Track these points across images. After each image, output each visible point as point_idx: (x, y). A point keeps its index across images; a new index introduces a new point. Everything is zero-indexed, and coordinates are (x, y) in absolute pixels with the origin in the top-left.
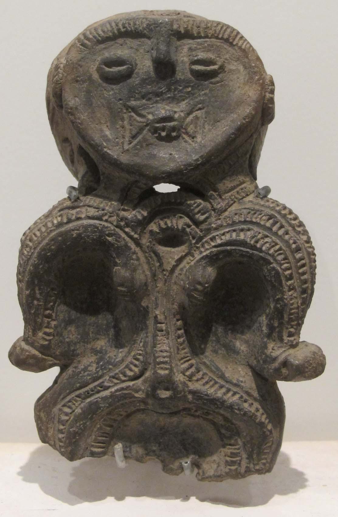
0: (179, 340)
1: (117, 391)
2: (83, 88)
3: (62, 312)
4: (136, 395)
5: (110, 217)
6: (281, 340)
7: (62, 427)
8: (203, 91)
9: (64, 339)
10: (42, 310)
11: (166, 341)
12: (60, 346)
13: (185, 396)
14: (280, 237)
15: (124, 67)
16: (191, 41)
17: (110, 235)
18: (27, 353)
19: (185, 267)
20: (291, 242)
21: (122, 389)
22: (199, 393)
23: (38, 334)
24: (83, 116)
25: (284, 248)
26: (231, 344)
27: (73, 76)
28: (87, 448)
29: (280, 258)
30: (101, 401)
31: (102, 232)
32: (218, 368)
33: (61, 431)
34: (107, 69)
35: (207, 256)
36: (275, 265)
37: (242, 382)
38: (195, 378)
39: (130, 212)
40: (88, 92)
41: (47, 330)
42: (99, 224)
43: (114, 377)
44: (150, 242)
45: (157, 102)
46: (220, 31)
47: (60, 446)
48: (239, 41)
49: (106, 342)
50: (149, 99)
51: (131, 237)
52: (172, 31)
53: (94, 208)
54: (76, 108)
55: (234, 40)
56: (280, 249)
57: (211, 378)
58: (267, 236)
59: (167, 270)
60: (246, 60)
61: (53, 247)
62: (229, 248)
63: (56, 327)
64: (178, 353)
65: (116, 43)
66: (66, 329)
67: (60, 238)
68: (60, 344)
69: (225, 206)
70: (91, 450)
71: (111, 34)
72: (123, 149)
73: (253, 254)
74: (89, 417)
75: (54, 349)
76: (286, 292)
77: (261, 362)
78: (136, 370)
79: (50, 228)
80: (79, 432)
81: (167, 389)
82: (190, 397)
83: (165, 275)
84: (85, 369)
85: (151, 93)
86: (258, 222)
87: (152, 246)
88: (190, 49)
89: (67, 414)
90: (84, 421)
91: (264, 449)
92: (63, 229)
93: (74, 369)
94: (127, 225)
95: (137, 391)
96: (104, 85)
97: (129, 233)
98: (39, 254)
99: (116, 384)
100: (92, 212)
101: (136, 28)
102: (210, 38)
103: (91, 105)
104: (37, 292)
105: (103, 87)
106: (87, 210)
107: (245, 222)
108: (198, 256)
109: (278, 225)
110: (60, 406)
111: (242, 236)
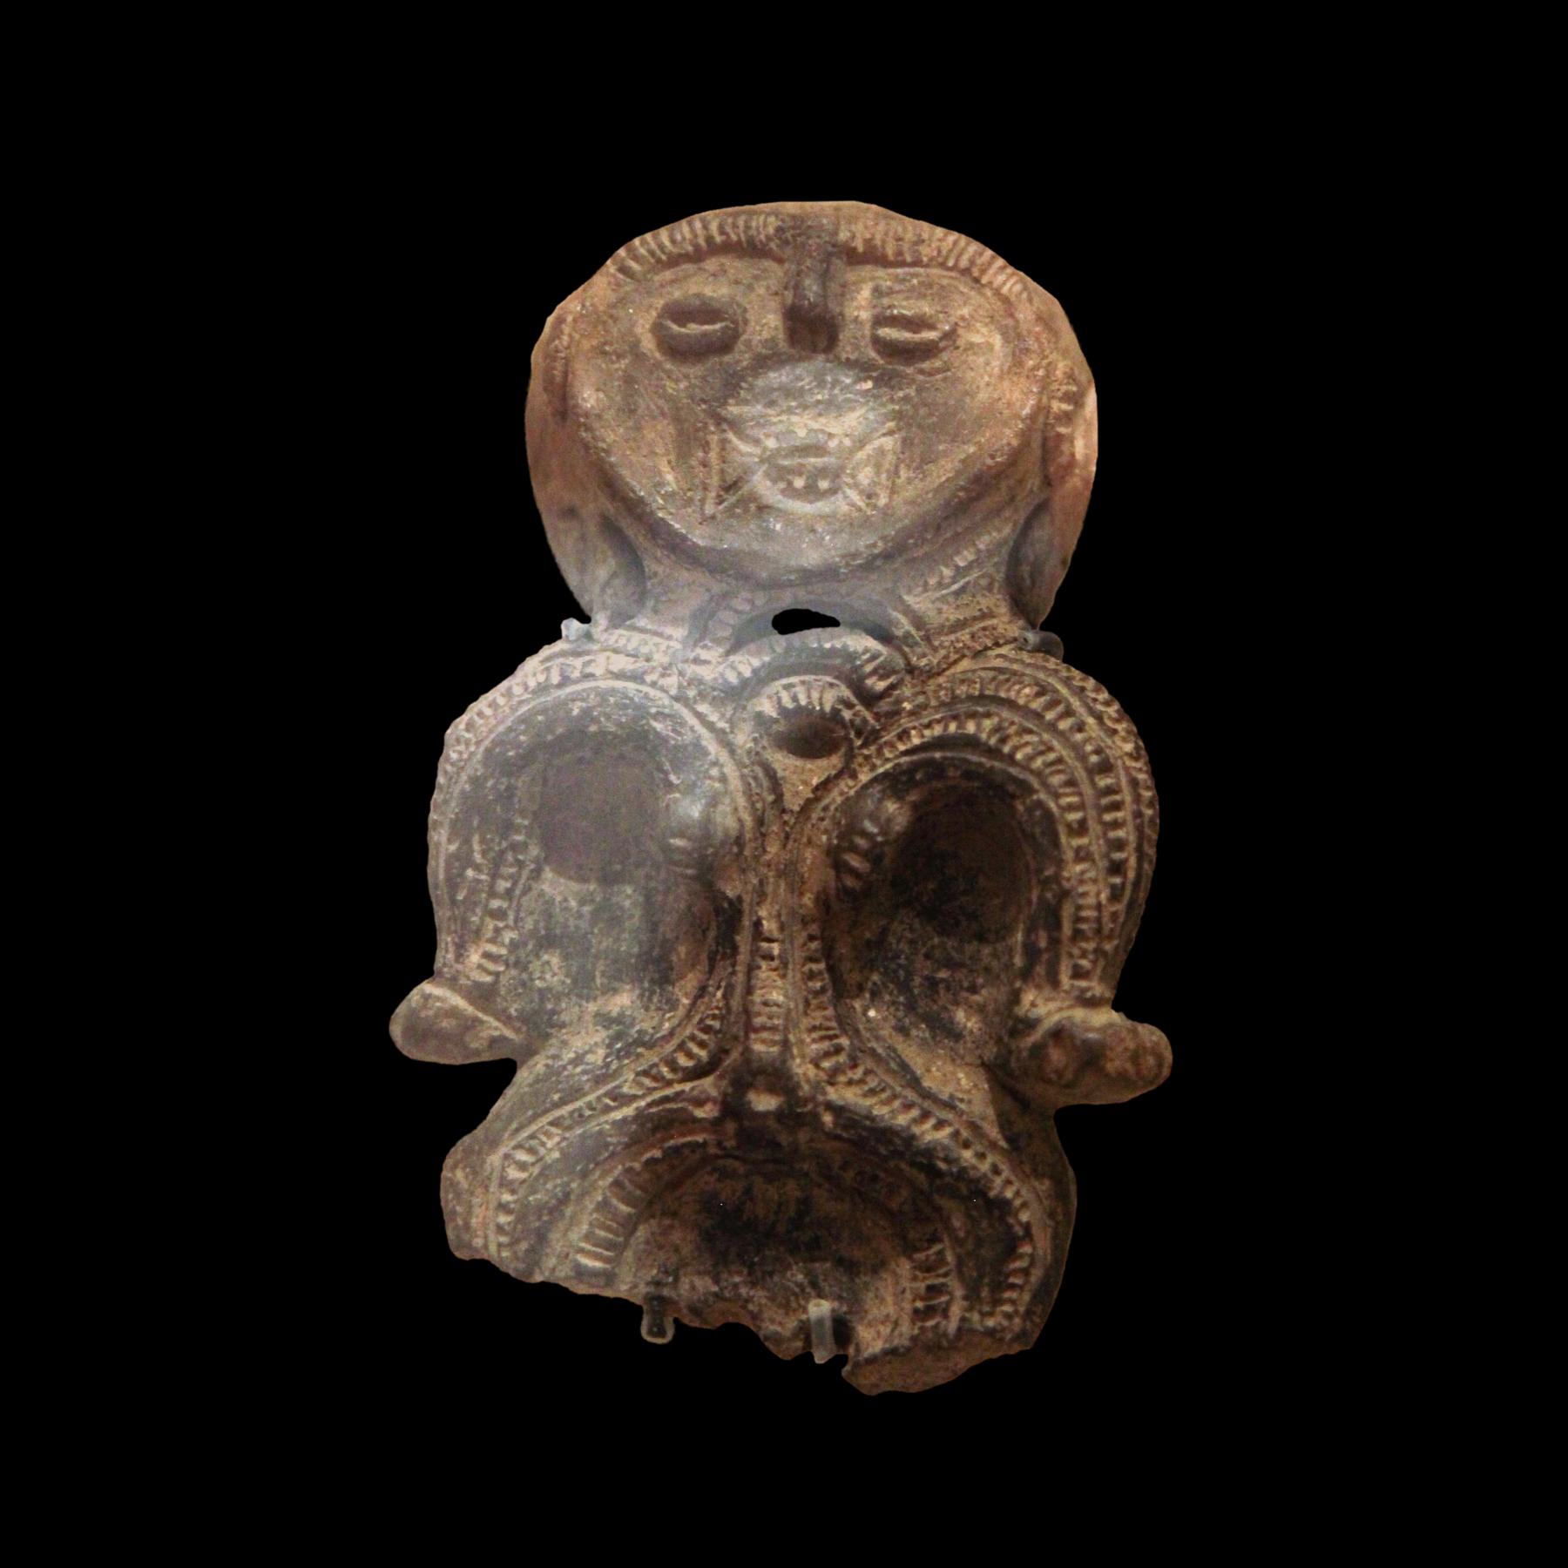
0: (810, 984)
1: (649, 1105)
2: (617, 370)
3: (532, 913)
4: (700, 1113)
5: (663, 675)
6: (1055, 983)
7: (507, 1197)
8: (902, 389)
9: (532, 980)
10: (484, 895)
11: (779, 983)
12: (520, 994)
13: (816, 1116)
14: (1061, 734)
15: (718, 326)
16: (881, 272)
17: (659, 716)
18: (438, 1004)
19: (834, 800)
20: (1089, 748)
21: (666, 1099)
22: (850, 1111)
23: (468, 956)
24: (611, 435)
25: (1067, 759)
26: (944, 1015)
27: (595, 342)
28: (567, 1255)
29: (1056, 780)
30: (609, 1130)
31: (641, 711)
32: (904, 1066)
33: (503, 1207)
34: (675, 327)
35: (886, 775)
36: (1043, 796)
37: (962, 1100)
38: (842, 1079)
39: (711, 667)
40: (629, 380)
41: (493, 949)
42: (637, 690)
43: (645, 1073)
44: (755, 740)
45: (790, 411)
46: (950, 251)
47: (500, 1245)
48: (995, 274)
49: (634, 998)
50: (771, 404)
51: (710, 726)
52: (834, 246)
53: (628, 655)
54: (599, 416)
55: (983, 272)
56: (1060, 760)
57: (883, 1085)
58: (1030, 732)
59: (792, 811)
60: (1010, 322)
61: (522, 738)
62: (938, 755)
63: (514, 946)
64: (806, 1014)
65: (700, 269)
66: (538, 956)
67: (540, 718)
68: (520, 991)
69: (939, 663)
70: (576, 1261)
71: (690, 249)
72: (703, 514)
73: (992, 768)
74: (578, 1168)
75: (507, 1001)
76: (1068, 863)
77: (1006, 1039)
78: (703, 1054)
79: (518, 696)
80: (551, 1205)
81: (771, 1090)
82: (828, 1119)
83: (785, 823)
84: (578, 1060)
85: (775, 390)
86: (1013, 698)
87: (758, 749)
88: (877, 292)
89: (523, 1166)
90: (565, 1179)
91: (1008, 1276)
92: (547, 699)
93: (550, 1062)
94: (702, 695)
95: (699, 1103)
96: (668, 366)
97: (706, 715)
98: (488, 751)
99: (651, 1090)
100: (621, 663)
101: (752, 237)
102: (927, 266)
103: (632, 412)
104: (476, 847)
105: (665, 371)
106: (608, 658)
107: (982, 698)
108: (864, 777)
109: (1060, 708)
110: (509, 1148)
111: (971, 728)
